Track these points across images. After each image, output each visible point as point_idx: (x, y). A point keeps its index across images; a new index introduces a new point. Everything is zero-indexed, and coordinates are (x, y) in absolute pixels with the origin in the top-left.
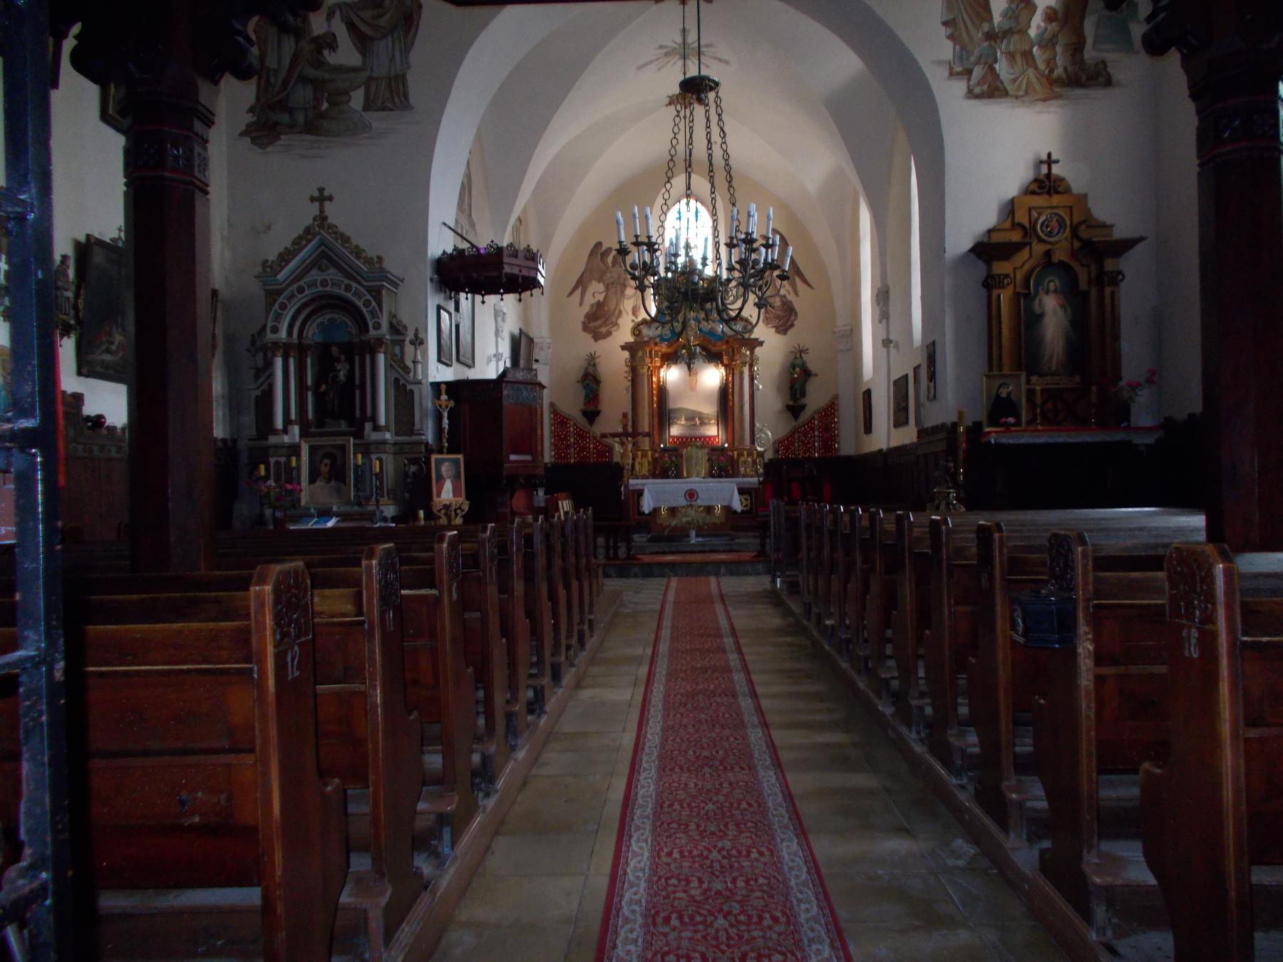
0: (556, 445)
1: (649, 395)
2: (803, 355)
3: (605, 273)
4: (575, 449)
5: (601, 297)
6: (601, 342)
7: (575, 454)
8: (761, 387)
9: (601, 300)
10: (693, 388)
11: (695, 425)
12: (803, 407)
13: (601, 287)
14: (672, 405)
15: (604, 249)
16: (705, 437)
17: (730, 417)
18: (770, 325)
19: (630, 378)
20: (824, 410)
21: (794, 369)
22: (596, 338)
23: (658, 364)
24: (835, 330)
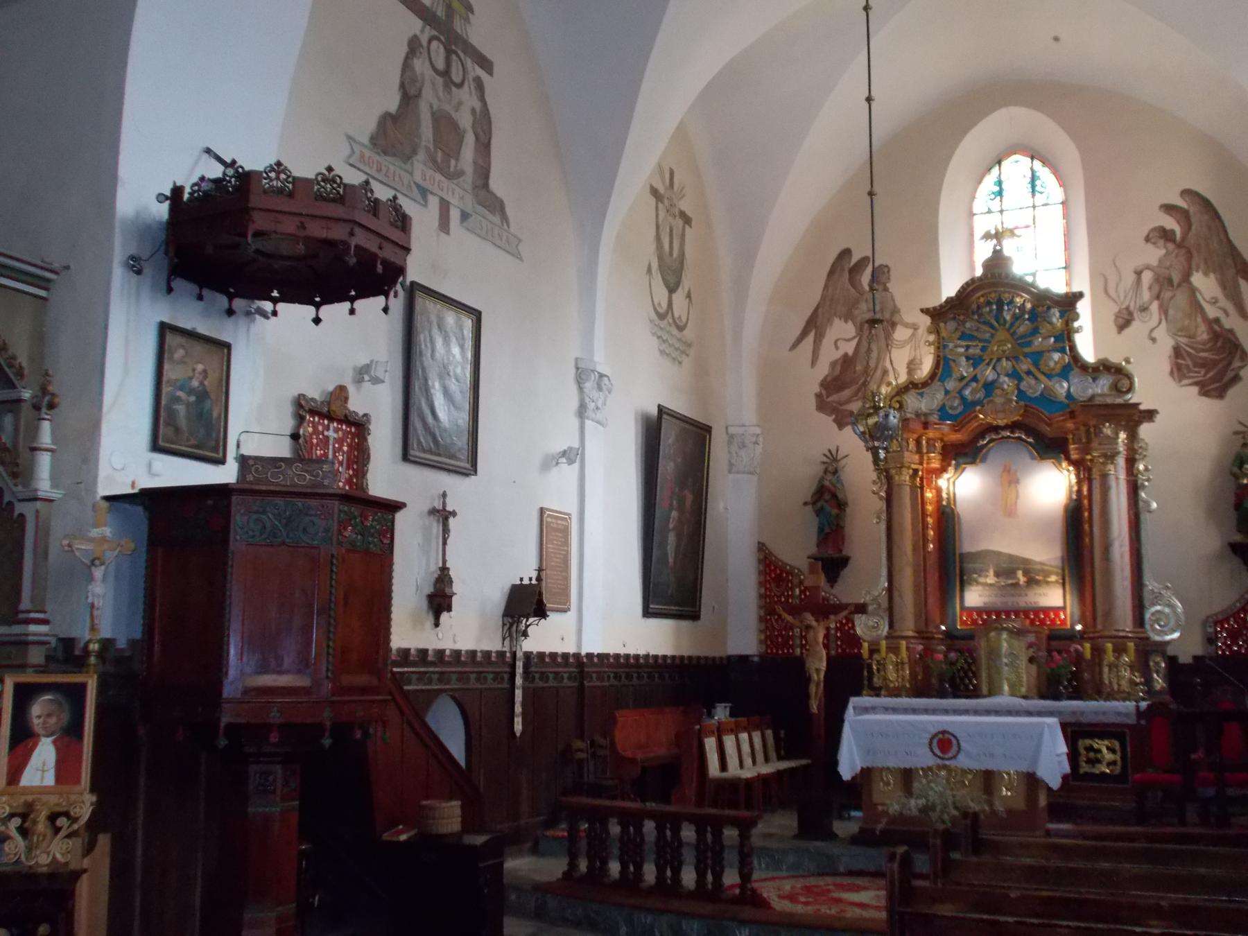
3: (855, 303)
5: (850, 348)
8: (1154, 505)
9: (850, 352)
10: (1010, 510)
11: (1016, 585)
13: (849, 329)
14: (968, 544)
15: (854, 260)
16: (1038, 611)
18: (1186, 382)
23: (936, 464)
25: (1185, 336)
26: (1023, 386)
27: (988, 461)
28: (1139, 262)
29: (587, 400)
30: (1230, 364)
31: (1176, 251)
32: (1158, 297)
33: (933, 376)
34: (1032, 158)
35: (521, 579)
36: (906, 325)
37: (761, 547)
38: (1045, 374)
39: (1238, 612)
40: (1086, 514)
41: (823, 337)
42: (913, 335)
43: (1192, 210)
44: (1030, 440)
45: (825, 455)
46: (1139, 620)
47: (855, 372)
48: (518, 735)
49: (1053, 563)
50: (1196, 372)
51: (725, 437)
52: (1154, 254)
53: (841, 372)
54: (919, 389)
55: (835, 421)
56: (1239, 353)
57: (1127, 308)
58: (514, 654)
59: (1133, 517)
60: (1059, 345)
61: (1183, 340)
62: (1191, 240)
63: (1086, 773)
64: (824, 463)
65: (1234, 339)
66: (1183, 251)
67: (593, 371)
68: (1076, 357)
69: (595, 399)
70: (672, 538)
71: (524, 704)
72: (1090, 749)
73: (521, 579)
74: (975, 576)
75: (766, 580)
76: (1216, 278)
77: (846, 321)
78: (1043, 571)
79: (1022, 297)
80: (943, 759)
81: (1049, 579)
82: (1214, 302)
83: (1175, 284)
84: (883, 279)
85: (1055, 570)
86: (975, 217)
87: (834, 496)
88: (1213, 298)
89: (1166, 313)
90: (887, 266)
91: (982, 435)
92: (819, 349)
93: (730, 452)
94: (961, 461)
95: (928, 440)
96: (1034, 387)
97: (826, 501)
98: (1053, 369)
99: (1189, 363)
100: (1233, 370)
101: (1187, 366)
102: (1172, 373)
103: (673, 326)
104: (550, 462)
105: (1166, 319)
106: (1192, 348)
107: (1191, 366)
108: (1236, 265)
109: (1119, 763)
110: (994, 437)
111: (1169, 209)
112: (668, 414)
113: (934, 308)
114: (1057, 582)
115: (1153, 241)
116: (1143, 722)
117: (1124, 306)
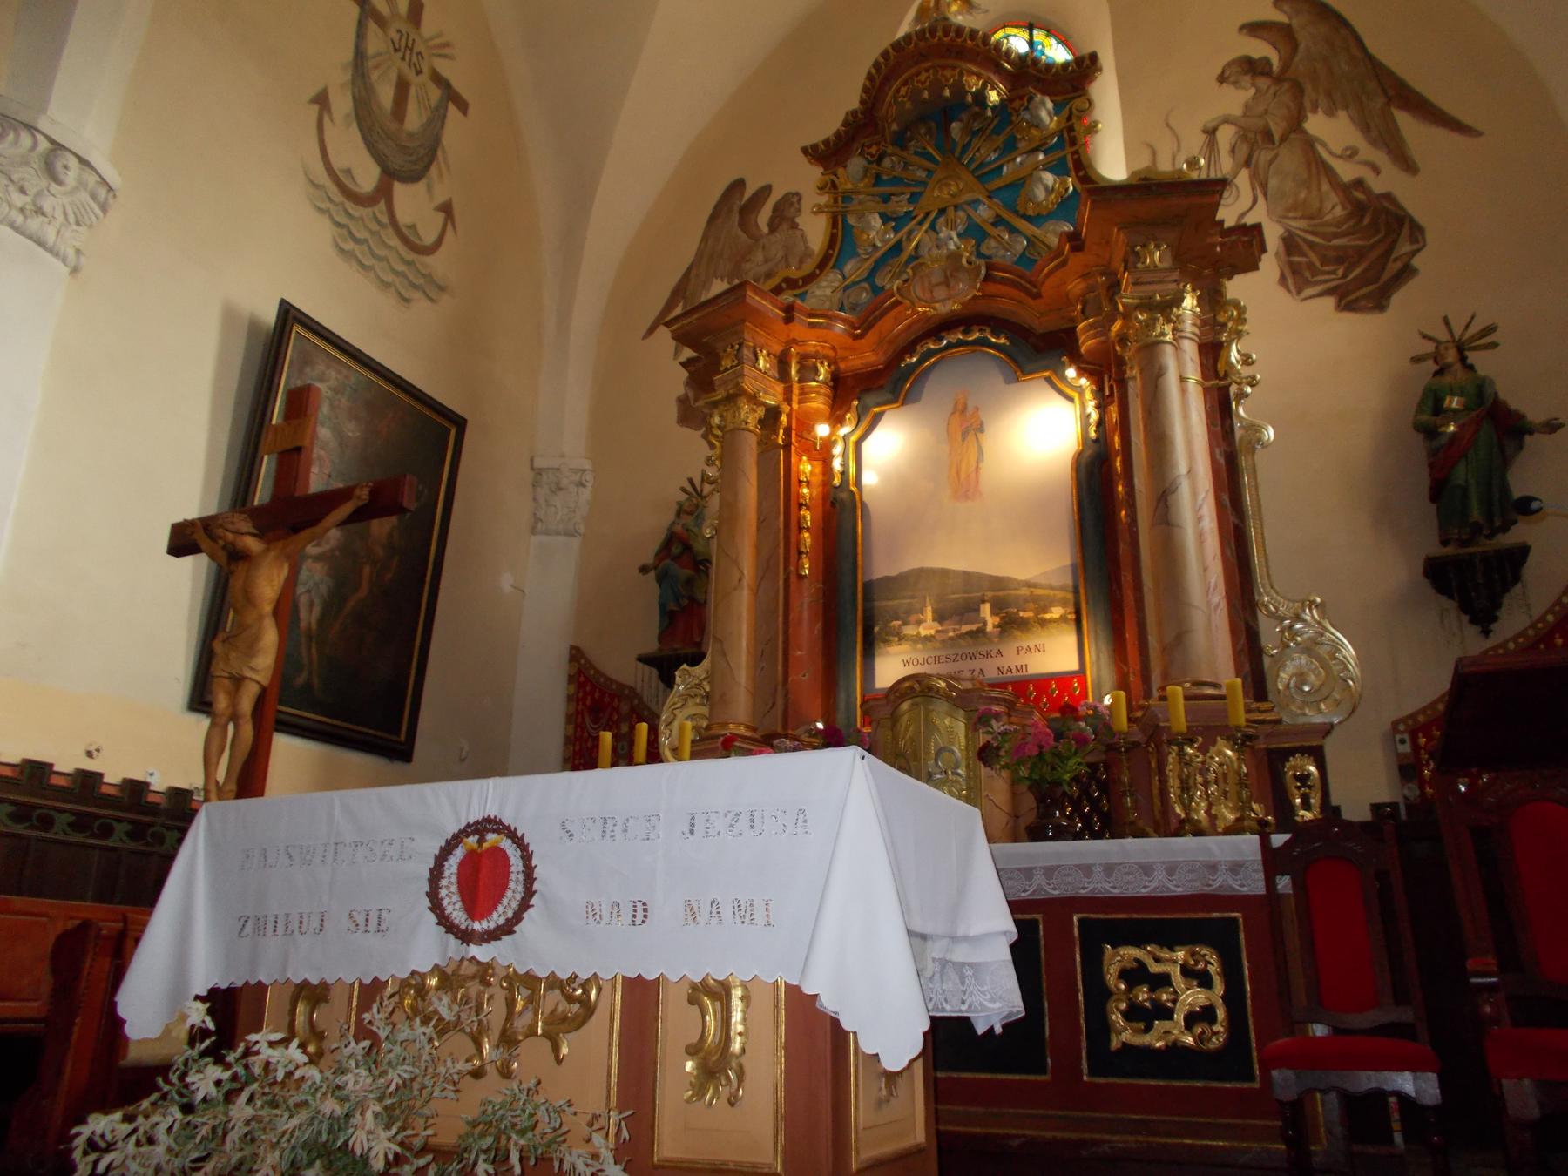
2: (1473, 357)
8: (1270, 434)
11: (981, 631)
14: (882, 565)
15: (749, 191)
17: (1127, 578)
18: (1309, 292)
21: (1438, 409)
25: (1302, 217)
26: (989, 247)
27: (923, 399)
28: (1207, 117)
30: (1389, 251)
31: (1272, 90)
32: (1247, 163)
37: (576, 654)
43: (1295, 23)
45: (684, 490)
46: (1258, 686)
49: (1055, 582)
50: (1328, 273)
52: (1234, 100)
54: (799, 287)
56: (1406, 231)
59: (1222, 461)
61: (1302, 224)
63: (1126, 1046)
65: (1391, 207)
72: (1135, 975)
74: (897, 623)
76: (1352, 119)
78: (1035, 599)
80: (466, 937)
81: (1048, 616)
82: (1351, 154)
83: (1277, 138)
85: (1060, 594)
87: (687, 547)
88: (1347, 149)
89: (1264, 187)
94: (870, 399)
95: (803, 358)
96: (1006, 248)
99: (1314, 259)
100: (1396, 260)
101: (1310, 266)
102: (1283, 280)
103: (390, 231)
105: (1265, 195)
106: (1312, 233)
107: (1318, 264)
108: (1385, 91)
109: (1221, 1013)
111: (1254, 29)
114: (1063, 619)
115: (1232, 79)
116: (1284, 883)
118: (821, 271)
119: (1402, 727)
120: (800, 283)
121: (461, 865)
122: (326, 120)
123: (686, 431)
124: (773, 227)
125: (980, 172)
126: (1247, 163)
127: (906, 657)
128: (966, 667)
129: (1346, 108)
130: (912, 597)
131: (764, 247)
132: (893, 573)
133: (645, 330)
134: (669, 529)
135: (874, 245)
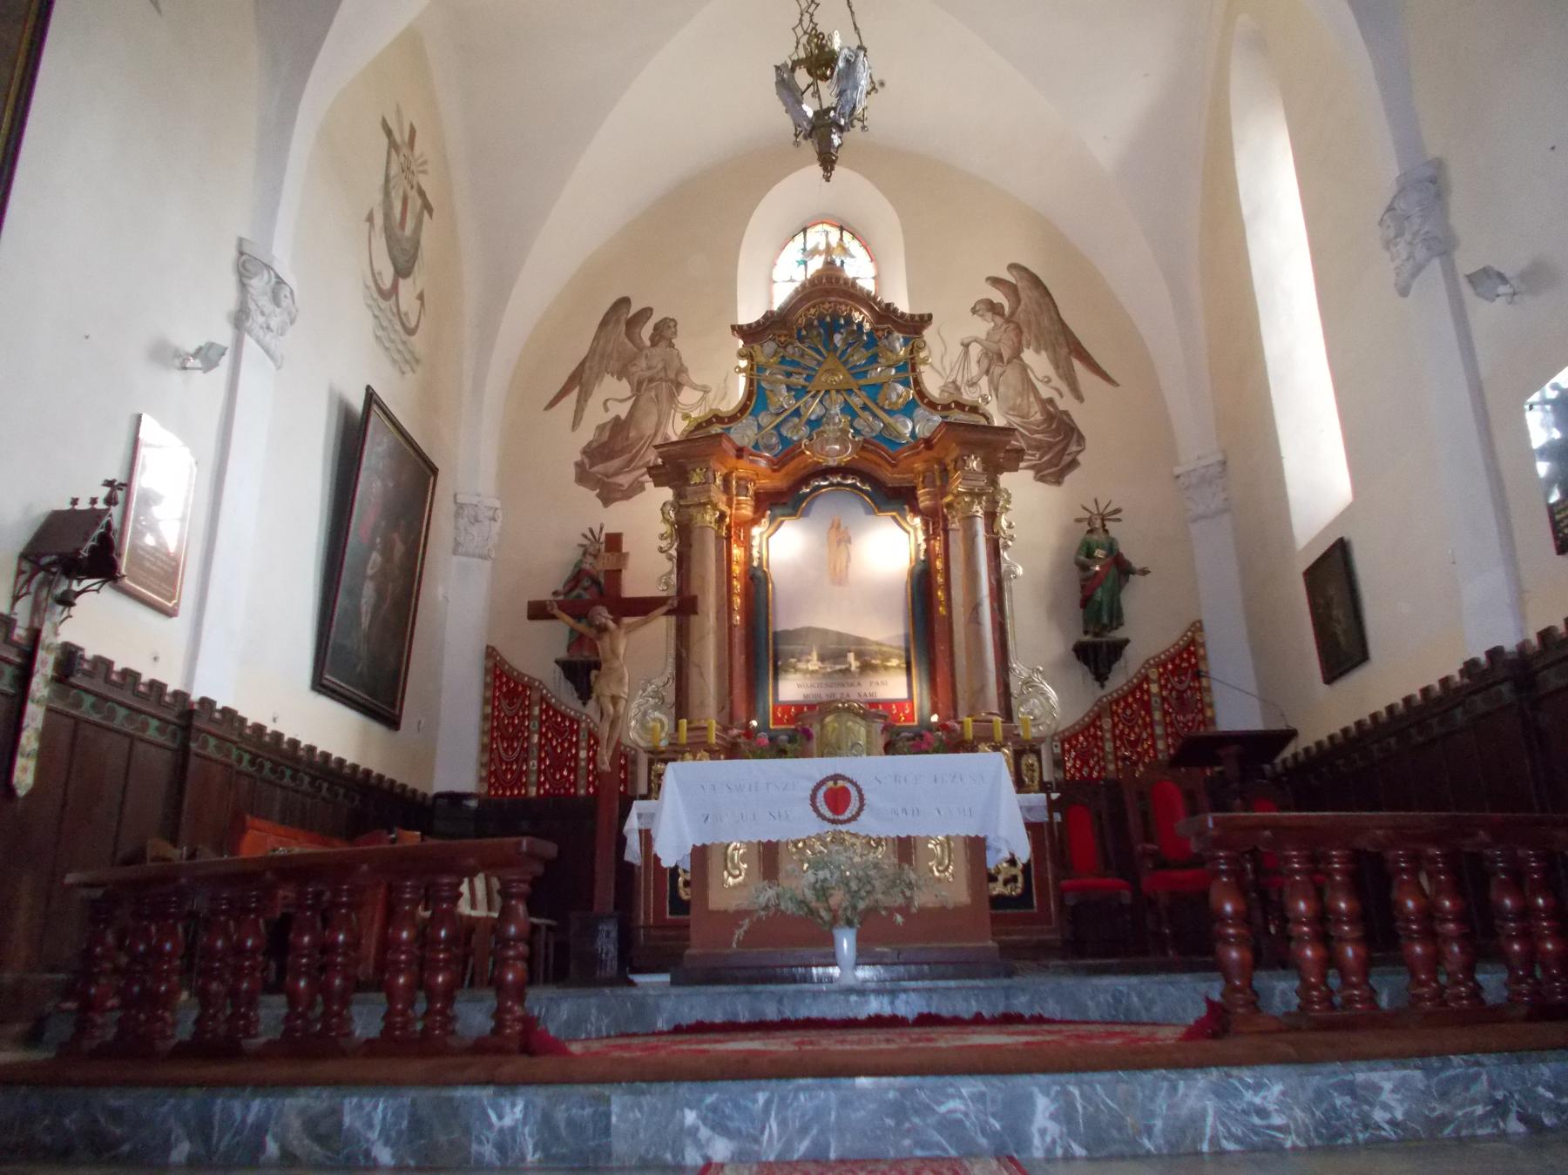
0: (492, 750)
1: (719, 587)
2: (1109, 525)
3: (632, 360)
4: (541, 761)
5: (622, 410)
6: (619, 507)
7: (539, 771)
9: (623, 416)
11: (847, 671)
12: (1118, 648)
13: (624, 388)
14: (784, 620)
15: (634, 310)
17: (941, 648)
19: (673, 552)
20: (1172, 660)
21: (1090, 555)
22: (607, 500)
23: (747, 511)
24: (1178, 470)
26: (858, 423)
27: (811, 516)
28: (966, 334)
29: (252, 306)
30: (1065, 449)
31: (1004, 326)
32: (987, 372)
33: (743, 409)
34: (842, 229)
35: (75, 501)
36: (695, 387)
37: (491, 652)
38: (882, 408)
39: (1088, 728)
40: (940, 580)
41: (590, 395)
42: (703, 398)
43: (1020, 285)
44: (867, 488)
45: (585, 536)
46: (1008, 713)
47: (627, 439)
48: (21, 792)
49: (895, 644)
51: (453, 508)
52: (982, 327)
53: (610, 437)
55: (599, 496)
56: (1075, 436)
57: (954, 382)
58: (35, 635)
59: (994, 582)
60: (902, 375)
61: (1018, 420)
62: (1021, 316)
64: (582, 546)
65: (1068, 421)
66: (1012, 326)
67: (269, 267)
68: (921, 394)
69: (266, 311)
70: (368, 591)
71: (45, 736)
73: (75, 501)
74: (793, 660)
75: (494, 697)
77: (619, 379)
79: (861, 313)
80: (833, 822)
81: (889, 664)
82: (1048, 381)
83: (1005, 360)
84: (668, 333)
85: (897, 651)
86: (775, 286)
90: (673, 320)
91: (805, 480)
92: (583, 410)
93: (456, 528)
94: (778, 511)
95: (739, 479)
96: (870, 425)
97: (585, 589)
98: (896, 403)
100: (1069, 454)
103: (397, 317)
104: (166, 355)
106: (1024, 428)
109: (1020, 879)
110: (822, 483)
111: (996, 282)
112: (377, 404)
113: (749, 326)
114: (898, 667)
116: (1058, 817)
117: (950, 380)
118: (742, 415)
119: (1056, 738)
120: (726, 420)
121: (825, 794)
122: (372, 234)
123: (583, 489)
124: (654, 343)
125: (854, 371)
126: (987, 372)
127: (799, 682)
128: (839, 692)
129: (1046, 350)
130: (804, 645)
131: (646, 357)
132: (791, 628)
133: (545, 404)
134: (576, 566)
135: (782, 407)
